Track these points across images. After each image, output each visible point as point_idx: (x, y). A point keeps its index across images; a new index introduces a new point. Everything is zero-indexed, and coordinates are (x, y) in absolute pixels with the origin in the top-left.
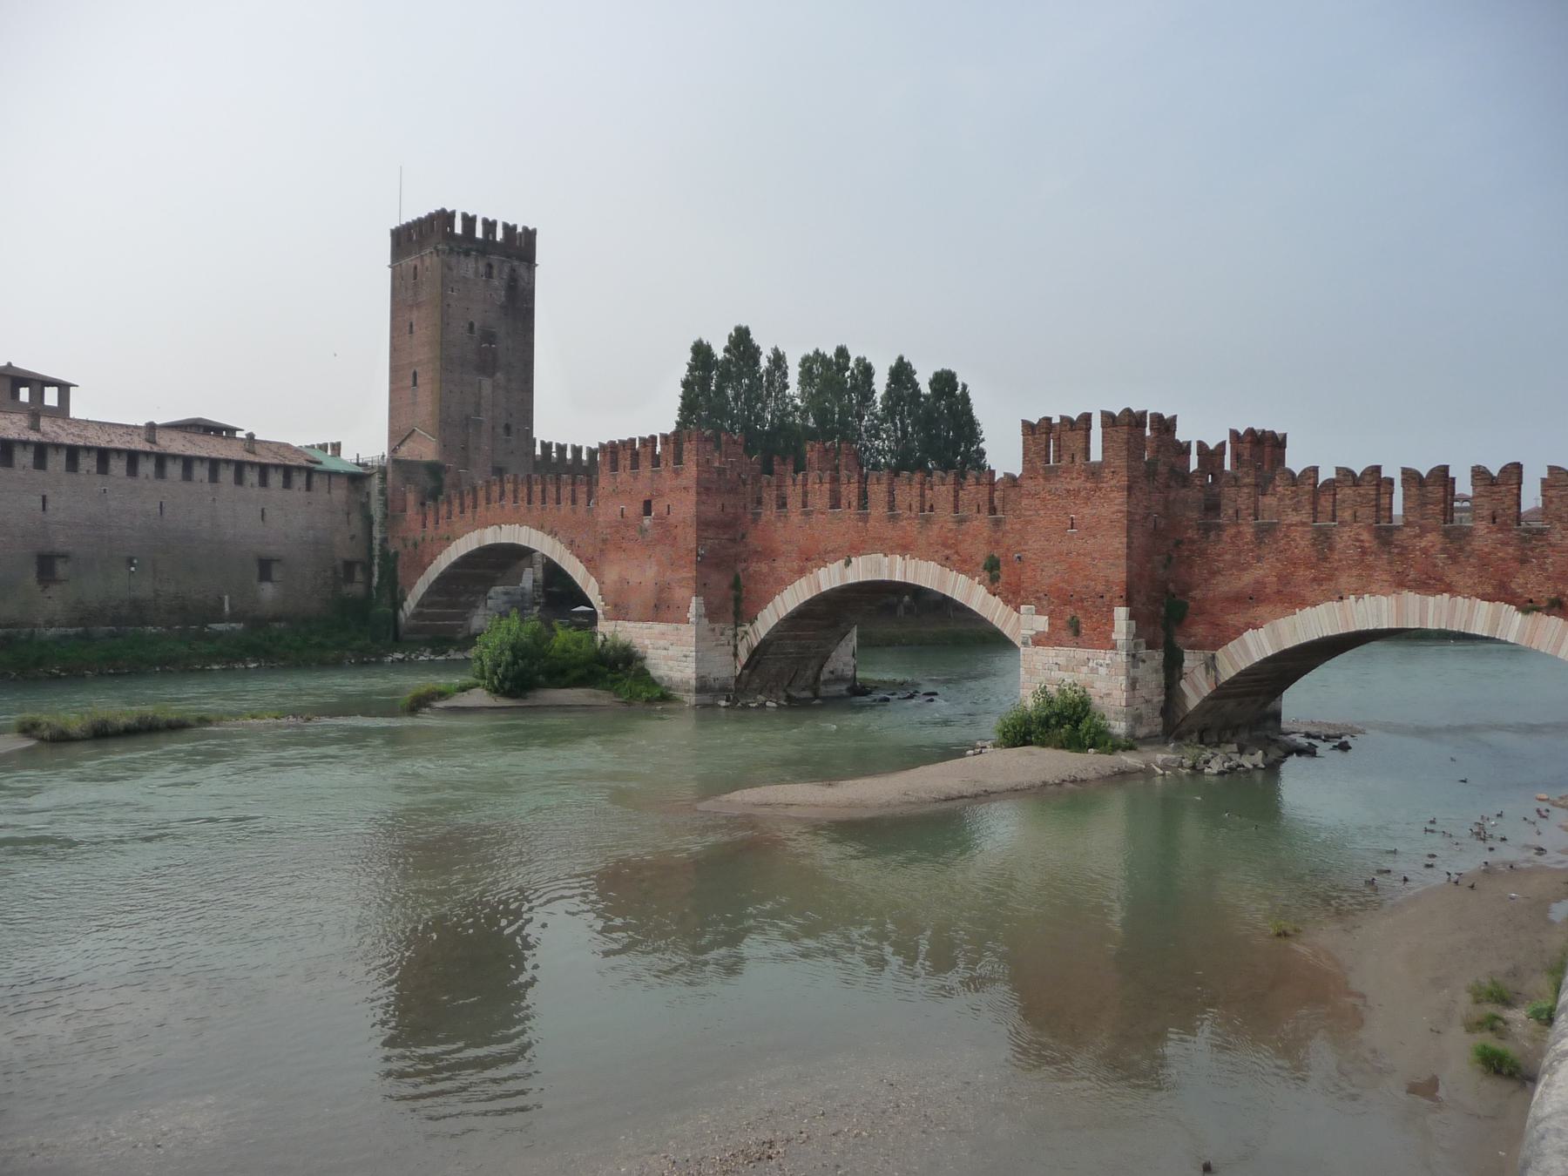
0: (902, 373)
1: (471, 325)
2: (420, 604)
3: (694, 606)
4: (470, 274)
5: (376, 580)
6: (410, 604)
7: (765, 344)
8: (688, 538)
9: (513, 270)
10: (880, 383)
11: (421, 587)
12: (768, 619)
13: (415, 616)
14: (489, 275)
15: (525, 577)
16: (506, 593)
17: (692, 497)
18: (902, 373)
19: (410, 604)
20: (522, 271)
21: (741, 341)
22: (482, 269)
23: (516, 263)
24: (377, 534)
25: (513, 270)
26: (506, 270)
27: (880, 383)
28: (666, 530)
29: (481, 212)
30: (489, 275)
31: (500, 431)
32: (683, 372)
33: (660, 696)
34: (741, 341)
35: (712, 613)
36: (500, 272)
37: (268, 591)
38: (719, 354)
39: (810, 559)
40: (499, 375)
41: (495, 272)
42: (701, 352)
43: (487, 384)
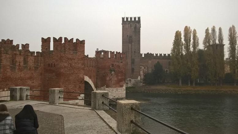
1: (128, 35)
4: (127, 27)
9: (136, 25)
14: (131, 27)
15: (139, 78)
16: (135, 81)
20: (137, 25)
22: (129, 25)
23: (136, 23)
25: (136, 25)
26: (134, 25)
29: (129, 16)
30: (131, 27)
31: (133, 53)
36: (133, 25)
40: (133, 43)
41: (132, 26)
43: (130, 45)
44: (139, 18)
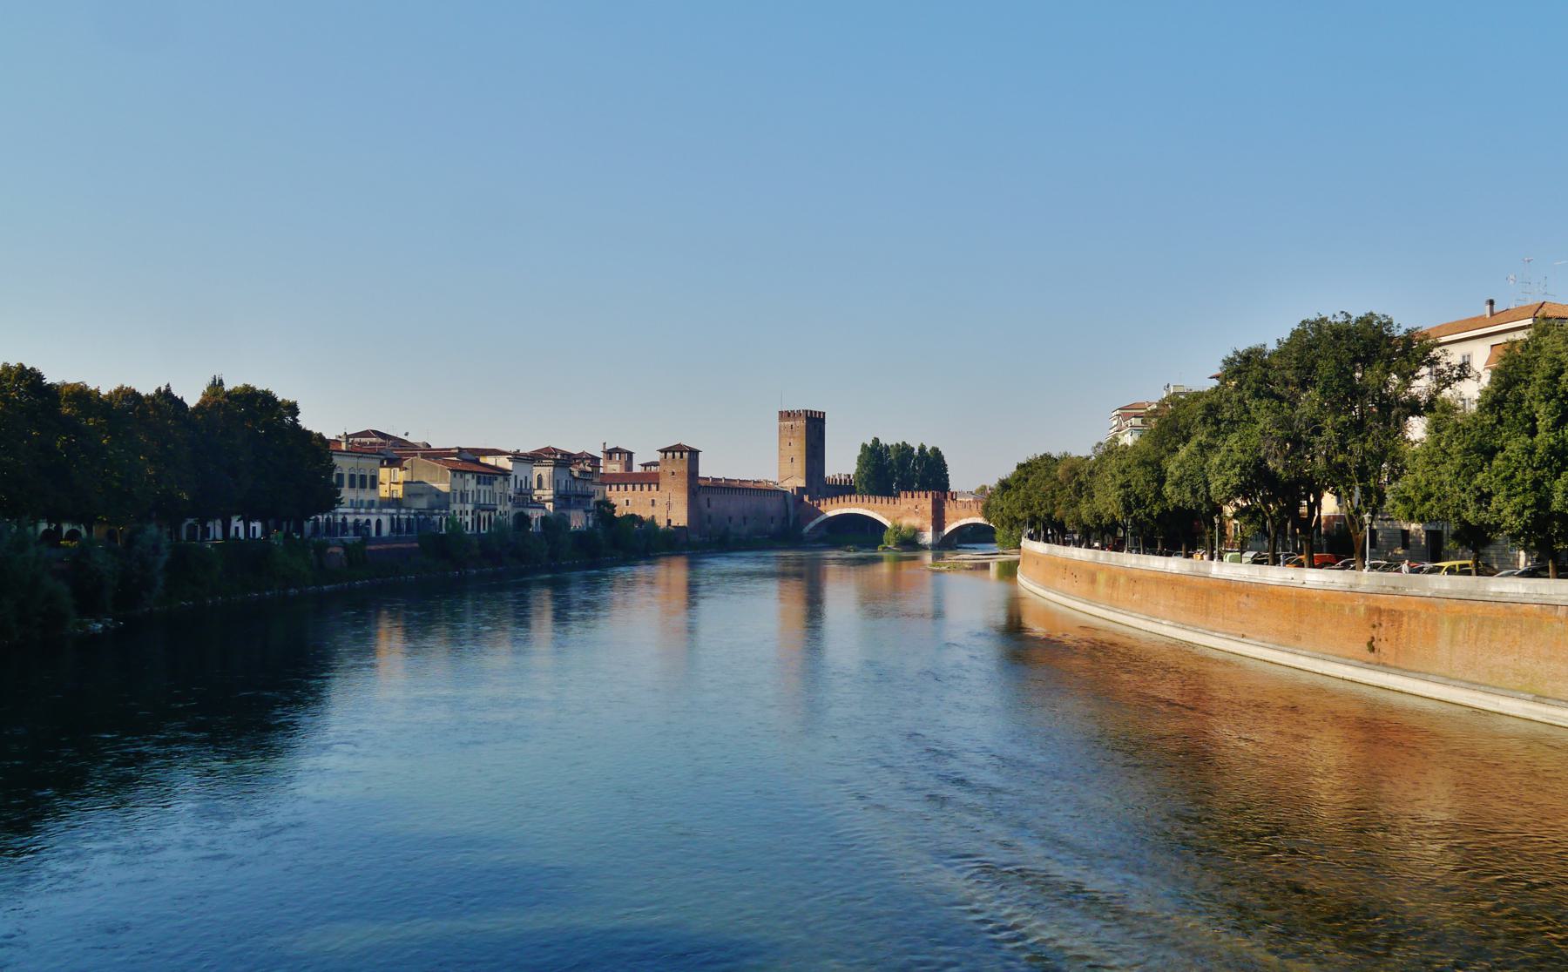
0: (922, 449)
2: (811, 530)
3: (931, 528)
5: (791, 522)
6: (806, 530)
7: (883, 442)
8: (930, 513)
10: (916, 451)
11: (812, 525)
12: (947, 531)
13: (808, 533)
17: (931, 505)
18: (922, 449)
19: (806, 530)
21: (876, 441)
24: (791, 509)
27: (916, 451)
28: (923, 511)
32: (859, 453)
33: (924, 548)
34: (876, 441)
35: (934, 530)
37: (773, 526)
38: (869, 445)
39: (958, 518)
42: (864, 446)
44: (824, 413)
